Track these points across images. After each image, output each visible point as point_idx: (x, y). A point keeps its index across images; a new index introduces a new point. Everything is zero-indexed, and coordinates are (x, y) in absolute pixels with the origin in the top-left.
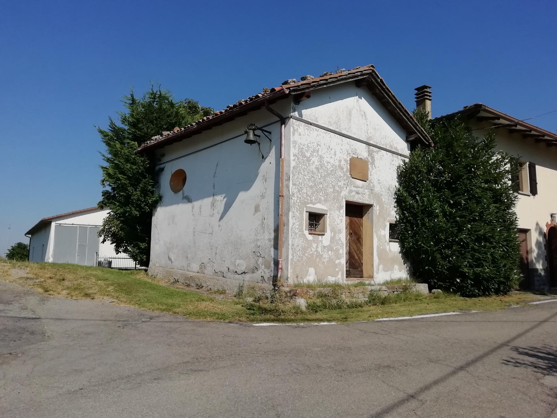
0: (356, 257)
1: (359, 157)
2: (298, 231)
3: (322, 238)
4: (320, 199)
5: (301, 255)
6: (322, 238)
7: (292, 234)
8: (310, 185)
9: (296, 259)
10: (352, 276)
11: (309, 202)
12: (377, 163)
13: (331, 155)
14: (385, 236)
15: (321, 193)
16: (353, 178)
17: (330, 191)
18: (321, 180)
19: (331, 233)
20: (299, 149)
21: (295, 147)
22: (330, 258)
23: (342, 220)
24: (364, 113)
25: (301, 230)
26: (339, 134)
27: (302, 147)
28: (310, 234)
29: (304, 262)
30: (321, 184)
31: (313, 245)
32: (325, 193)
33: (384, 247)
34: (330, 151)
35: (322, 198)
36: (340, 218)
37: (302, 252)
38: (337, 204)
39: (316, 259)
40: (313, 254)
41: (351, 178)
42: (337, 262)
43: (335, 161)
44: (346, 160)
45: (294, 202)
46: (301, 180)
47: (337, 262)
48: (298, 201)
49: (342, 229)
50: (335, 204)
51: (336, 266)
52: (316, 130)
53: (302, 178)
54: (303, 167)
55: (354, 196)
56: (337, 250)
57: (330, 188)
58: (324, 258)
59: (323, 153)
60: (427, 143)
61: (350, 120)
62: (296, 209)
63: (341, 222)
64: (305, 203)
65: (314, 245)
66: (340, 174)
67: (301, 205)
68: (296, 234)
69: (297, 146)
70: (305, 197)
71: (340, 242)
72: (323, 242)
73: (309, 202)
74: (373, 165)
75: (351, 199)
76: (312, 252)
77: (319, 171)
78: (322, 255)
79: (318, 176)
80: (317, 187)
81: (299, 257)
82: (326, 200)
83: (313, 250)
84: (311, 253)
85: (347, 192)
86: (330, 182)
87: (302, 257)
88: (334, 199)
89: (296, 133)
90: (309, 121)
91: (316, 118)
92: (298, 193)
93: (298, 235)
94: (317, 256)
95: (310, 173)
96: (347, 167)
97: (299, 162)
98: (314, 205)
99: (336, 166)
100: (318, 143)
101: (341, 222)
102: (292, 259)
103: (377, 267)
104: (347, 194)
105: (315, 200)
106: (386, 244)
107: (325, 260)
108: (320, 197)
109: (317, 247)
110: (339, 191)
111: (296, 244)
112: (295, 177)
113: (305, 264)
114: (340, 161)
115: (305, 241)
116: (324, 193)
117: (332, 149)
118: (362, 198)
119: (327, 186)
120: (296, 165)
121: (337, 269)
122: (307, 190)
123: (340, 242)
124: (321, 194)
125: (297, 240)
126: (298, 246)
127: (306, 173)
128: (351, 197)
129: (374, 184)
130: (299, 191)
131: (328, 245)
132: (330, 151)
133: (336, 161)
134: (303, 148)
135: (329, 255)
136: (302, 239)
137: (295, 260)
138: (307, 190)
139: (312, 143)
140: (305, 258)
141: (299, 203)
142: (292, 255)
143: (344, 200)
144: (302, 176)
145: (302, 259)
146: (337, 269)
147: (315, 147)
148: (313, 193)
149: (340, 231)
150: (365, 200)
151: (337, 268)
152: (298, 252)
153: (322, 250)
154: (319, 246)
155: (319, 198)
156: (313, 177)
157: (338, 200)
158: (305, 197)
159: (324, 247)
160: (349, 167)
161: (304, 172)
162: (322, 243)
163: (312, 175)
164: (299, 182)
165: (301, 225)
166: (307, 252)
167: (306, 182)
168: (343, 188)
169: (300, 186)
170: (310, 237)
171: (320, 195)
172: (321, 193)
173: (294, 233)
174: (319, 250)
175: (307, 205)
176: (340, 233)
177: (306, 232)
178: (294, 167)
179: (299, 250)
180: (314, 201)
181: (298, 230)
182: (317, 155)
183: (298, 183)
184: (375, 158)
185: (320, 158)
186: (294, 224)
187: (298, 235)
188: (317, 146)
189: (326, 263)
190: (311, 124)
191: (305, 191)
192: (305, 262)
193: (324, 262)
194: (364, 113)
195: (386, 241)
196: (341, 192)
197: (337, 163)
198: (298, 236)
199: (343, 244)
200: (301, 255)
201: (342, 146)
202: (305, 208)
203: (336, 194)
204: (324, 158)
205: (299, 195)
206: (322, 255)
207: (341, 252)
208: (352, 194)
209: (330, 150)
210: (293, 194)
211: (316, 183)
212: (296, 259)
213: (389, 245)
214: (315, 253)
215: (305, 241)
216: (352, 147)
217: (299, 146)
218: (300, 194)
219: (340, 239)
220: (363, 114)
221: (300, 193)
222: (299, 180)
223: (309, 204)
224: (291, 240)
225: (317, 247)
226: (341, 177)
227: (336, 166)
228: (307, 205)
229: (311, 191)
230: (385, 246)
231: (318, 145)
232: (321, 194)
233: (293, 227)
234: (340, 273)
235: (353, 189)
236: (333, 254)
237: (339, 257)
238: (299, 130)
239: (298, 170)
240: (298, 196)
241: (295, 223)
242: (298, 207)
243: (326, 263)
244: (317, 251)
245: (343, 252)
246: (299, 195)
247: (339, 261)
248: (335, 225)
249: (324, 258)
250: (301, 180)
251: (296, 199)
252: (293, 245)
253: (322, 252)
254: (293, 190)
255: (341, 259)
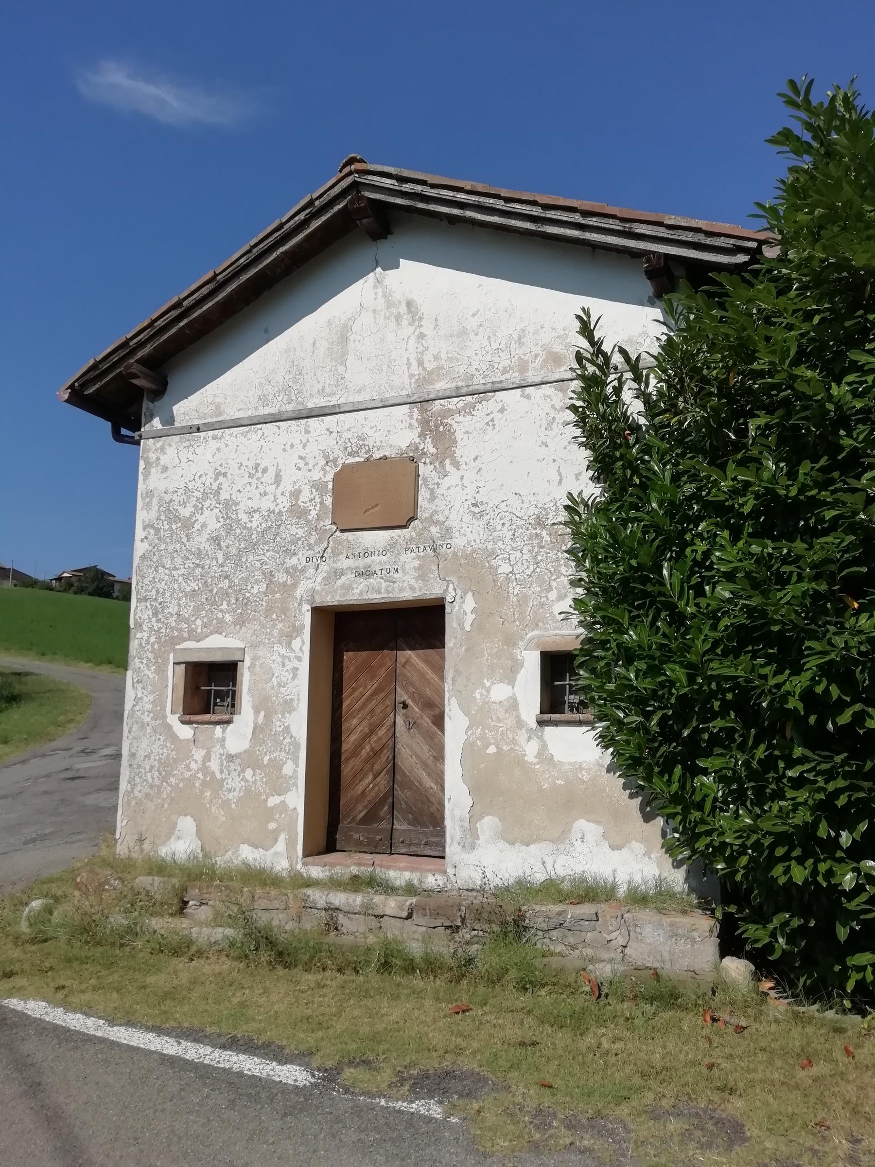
0: (417, 784)
1: (377, 455)
2: (149, 719)
3: (224, 731)
4: (221, 621)
5: (157, 782)
6: (224, 731)
7: (131, 728)
8: (188, 589)
9: (140, 791)
10: (403, 850)
11: (186, 635)
12: (464, 450)
13: (262, 489)
14: (513, 705)
15: (225, 603)
16: (343, 531)
17: (255, 591)
18: (226, 569)
19: (257, 712)
20: (160, 507)
21: (148, 505)
22: (248, 790)
23: (297, 669)
24: (409, 304)
25: (159, 715)
26: (293, 415)
27: (167, 498)
28: (183, 722)
29: (164, 800)
30: (227, 577)
31: (193, 752)
32: (237, 600)
33: (505, 748)
34: (258, 479)
35: (228, 618)
36: (289, 665)
37: (160, 774)
38: (280, 626)
39: (202, 792)
40: (193, 777)
41: (338, 534)
42: (273, 801)
43: (275, 499)
44: (318, 486)
45: (140, 645)
46: (163, 583)
47: (273, 801)
48: (153, 639)
49: (295, 698)
50: (274, 626)
51: (270, 814)
52: (214, 438)
53: (167, 578)
54: (171, 548)
55: (349, 588)
56: (276, 765)
57: (257, 582)
58: (229, 791)
59: (235, 489)
60: (742, 258)
61: (342, 359)
62: (145, 661)
63: (295, 677)
64: (174, 641)
65: (198, 754)
66: (293, 532)
67: (160, 649)
68: (143, 726)
69: (155, 501)
70: (173, 624)
71: (288, 740)
72: (228, 744)
73: (186, 635)
74: (448, 461)
75: (334, 598)
76: (189, 773)
77: (219, 545)
78: (223, 780)
79: (217, 559)
80: (211, 591)
81: (151, 787)
82: (241, 622)
83: (193, 766)
84: (187, 775)
85: (319, 580)
86: (258, 564)
87: (159, 787)
88: (269, 611)
89: (153, 470)
90: (196, 422)
91: (218, 406)
92: (154, 619)
93: (149, 730)
94: (204, 784)
95: (191, 557)
96: (322, 503)
97: (159, 539)
98: (198, 641)
99: (280, 513)
100: (220, 468)
101: (294, 678)
102: (129, 793)
103: (467, 824)
104: (318, 588)
105: (205, 625)
106: (522, 736)
107: (230, 796)
108: (220, 615)
109: (207, 758)
110: (289, 582)
111: (141, 753)
112: (146, 581)
113: (166, 805)
114: (296, 494)
115: (169, 745)
116: (233, 601)
117: (265, 470)
118: (384, 585)
119: (246, 580)
120: (150, 548)
121: (272, 826)
122: (179, 605)
123: (288, 740)
124: (224, 606)
125: (145, 743)
126: (147, 757)
127: (179, 561)
128: (335, 591)
129: (453, 522)
130: (155, 614)
131: (245, 752)
132: (258, 479)
133: (281, 499)
134: (171, 501)
135: (247, 781)
136: (162, 738)
137: (137, 794)
138: (179, 605)
139: (200, 476)
140: (167, 790)
141: (153, 644)
142: (129, 782)
143: (306, 608)
144: (167, 571)
145: (160, 793)
146: (272, 826)
147: (207, 484)
148: (196, 611)
149: (289, 706)
150: (401, 590)
151: (274, 820)
152: (149, 775)
153: (222, 765)
154: (213, 756)
155: (217, 619)
156: (198, 566)
157: (284, 610)
158: (173, 624)
159: (231, 758)
160: (329, 501)
161: (173, 559)
162: (223, 746)
163: (198, 562)
164: (158, 592)
165: (159, 702)
166: (176, 772)
167: (176, 586)
168: (303, 570)
169: (160, 600)
170: (185, 732)
171: (221, 611)
172: (225, 603)
173: (137, 723)
174: (214, 765)
175: (177, 647)
176: (289, 712)
177: (174, 720)
178: (143, 557)
179: (152, 767)
180: (199, 630)
181: (151, 715)
182: (214, 502)
183: (154, 593)
184: (459, 435)
185: (226, 507)
186: (137, 700)
187: (149, 730)
188: (216, 479)
189: (233, 806)
190: (198, 430)
191: (173, 609)
192: (168, 800)
193: (227, 802)
194: (409, 304)
195: (520, 723)
196: (295, 585)
197: (284, 503)
198: (148, 731)
199: (297, 746)
200: (157, 782)
201: (304, 447)
202: (171, 655)
203: (278, 596)
204: (237, 504)
205: (155, 624)
206: (223, 780)
207: (288, 769)
208: (339, 582)
209: (259, 475)
210: (139, 626)
211: (209, 581)
212: (140, 791)
213: (541, 738)
214: (200, 775)
215: (169, 745)
216: (348, 435)
217: (161, 499)
218: (158, 621)
219: (287, 729)
220: (403, 309)
221: (160, 616)
222: (158, 585)
223: (185, 640)
224: (129, 742)
225: (207, 758)
226: (299, 539)
227: (280, 513)
228: (177, 647)
229: (192, 604)
230: (514, 742)
231: (218, 475)
232: (224, 606)
233: (137, 708)
234: (282, 838)
235: (345, 563)
236: (258, 777)
237: (279, 787)
238: (164, 459)
239: (155, 560)
240: (151, 629)
241: (141, 698)
242: (151, 656)
243: (233, 806)
244: (205, 769)
245: (295, 772)
246: (155, 624)
247: (282, 798)
248: (273, 688)
249: (229, 791)
250: (163, 583)
251: (145, 635)
252: (133, 755)
253: (222, 772)
254: (139, 614)
255: (289, 794)
